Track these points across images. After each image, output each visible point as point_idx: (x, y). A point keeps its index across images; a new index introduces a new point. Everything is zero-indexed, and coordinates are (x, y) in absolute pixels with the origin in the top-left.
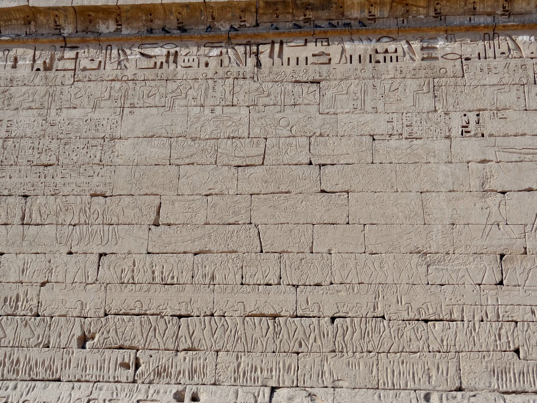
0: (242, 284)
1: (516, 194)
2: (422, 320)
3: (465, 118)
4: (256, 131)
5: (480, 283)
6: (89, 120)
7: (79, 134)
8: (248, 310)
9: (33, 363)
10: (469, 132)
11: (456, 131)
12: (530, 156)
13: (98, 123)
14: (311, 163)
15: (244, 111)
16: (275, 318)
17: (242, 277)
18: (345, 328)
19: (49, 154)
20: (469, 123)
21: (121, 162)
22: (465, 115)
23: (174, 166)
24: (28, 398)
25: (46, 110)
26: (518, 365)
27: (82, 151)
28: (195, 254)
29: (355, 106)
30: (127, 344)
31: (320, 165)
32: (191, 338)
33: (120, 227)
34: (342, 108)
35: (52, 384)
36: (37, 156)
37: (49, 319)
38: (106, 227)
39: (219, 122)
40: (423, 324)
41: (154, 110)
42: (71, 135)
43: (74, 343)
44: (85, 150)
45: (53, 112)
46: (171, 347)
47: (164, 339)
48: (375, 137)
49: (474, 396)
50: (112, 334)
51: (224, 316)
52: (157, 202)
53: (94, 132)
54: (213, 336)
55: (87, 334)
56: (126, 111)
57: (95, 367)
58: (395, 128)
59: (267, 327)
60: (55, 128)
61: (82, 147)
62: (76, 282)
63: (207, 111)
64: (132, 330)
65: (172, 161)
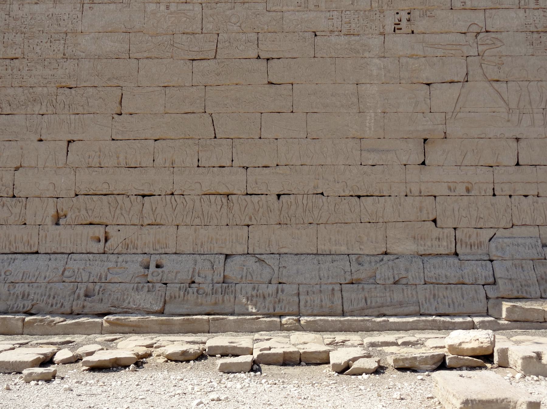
0: (198, 166)
1: (439, 85)
2: (356, 196)
3: (398, 16)
4: (209, 26)
5: (405, 163)
6: (51, 15)
7: (42, 29)
8: (204, 189)
9: (12, 238)
10: (401, 29)
11: (389, 28)
12: (453, 52)
13: (59, 18)
14: (259, 57)
15: (198, 8)
16: (228, 195)
17: (199, 160)
18: (289, 203)
19: (15, 48)
20: (400, 21)
21: (83, 55)
22: (397, 13)
23: (133, 60)
24: (10, 268)
25: (8, 6)
26: (436, 232)
27: (46, 45)
28: (156, 140)
29: (299, 4)
30: (96, 221)
31: (268, 59)
32: (153, 214)
33: (85, 116)
34: (287, 5)
35: (30, 256)
36: (4, 49)
37: (24, 199)
38: (73, 117)
39: (173, 19)
40: (356, 198)
41: (112, 6)
42: (34, 30)
43: (49, 221)
44: (49, 44)
45: (15, 7)
46: (136, 222)
47: (130, 216)
48: (317, 33)
49: (397, 258)
50: (83, 212)
51: (183, 195)
52: (118, 92)
53: (56, 27)
54: (174, 213)
55: (59, 211)
56: (86, 6)
57: (69, 241)
58: (335, 25)
59: (221, 203)
60: (19, 23)
61: (45, 41)
62: (47, 167)
63: (163, 8)
64: (101, 209)
65: (131, 55)
